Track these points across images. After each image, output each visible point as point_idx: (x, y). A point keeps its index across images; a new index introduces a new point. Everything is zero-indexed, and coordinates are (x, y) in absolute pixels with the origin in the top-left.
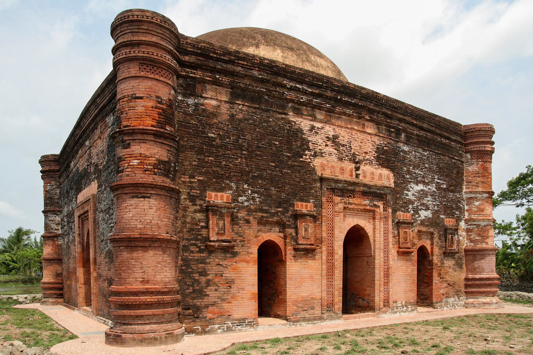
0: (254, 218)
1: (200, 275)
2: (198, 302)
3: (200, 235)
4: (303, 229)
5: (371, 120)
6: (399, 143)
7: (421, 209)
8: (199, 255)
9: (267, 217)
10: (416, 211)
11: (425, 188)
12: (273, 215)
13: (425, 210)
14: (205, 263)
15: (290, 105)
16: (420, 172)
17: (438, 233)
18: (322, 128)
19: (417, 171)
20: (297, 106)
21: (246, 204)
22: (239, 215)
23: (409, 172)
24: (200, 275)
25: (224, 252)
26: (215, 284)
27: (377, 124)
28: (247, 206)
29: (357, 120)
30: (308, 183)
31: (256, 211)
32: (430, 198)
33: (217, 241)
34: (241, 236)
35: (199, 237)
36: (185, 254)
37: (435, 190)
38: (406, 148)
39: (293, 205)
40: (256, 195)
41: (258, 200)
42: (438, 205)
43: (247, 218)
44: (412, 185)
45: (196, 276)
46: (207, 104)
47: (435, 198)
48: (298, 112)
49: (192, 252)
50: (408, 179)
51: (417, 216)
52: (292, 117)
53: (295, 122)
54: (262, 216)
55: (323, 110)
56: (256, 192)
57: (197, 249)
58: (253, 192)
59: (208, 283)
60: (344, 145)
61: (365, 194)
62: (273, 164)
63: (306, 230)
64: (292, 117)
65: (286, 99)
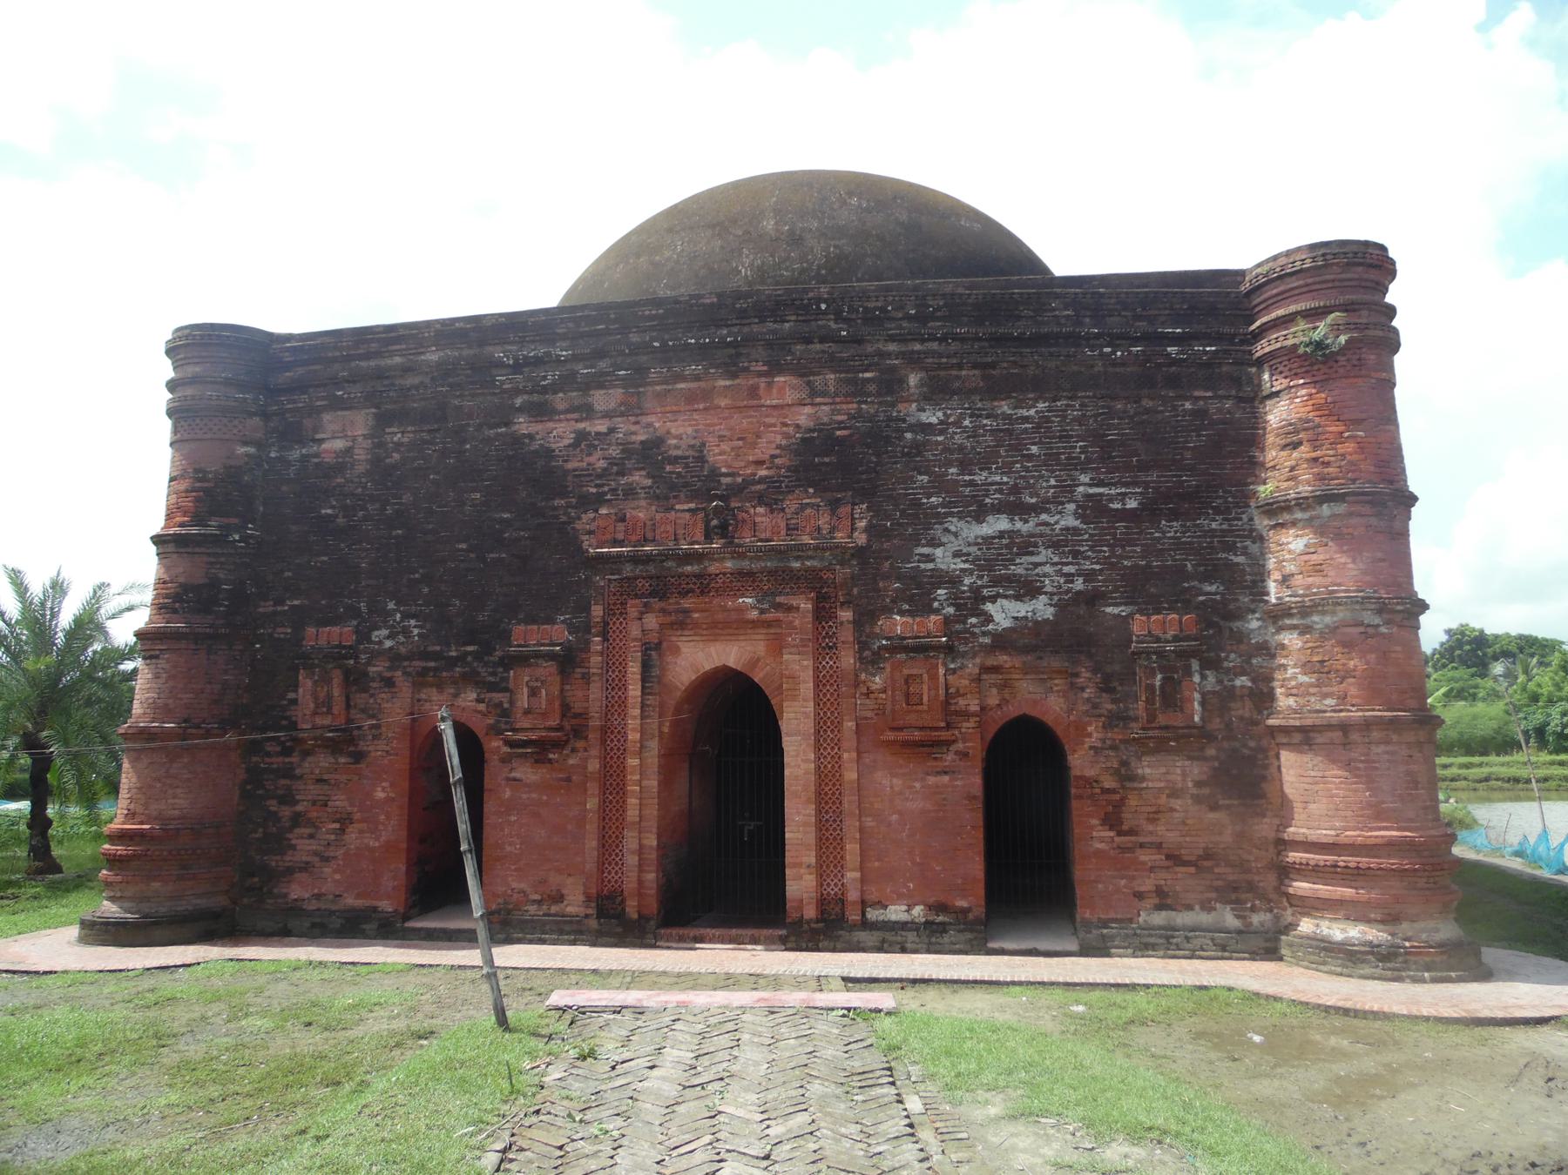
0: (405, 673)
1: (280, 803)
2: (273, 861)
3: (286, 718)
4: (525, 690)
5: (775, 368)
6: (901, 406)
7: (993, 599)
8: (280, 759)
9: (435, 669)
10: (973, 604)
11: (1019, 525)
12: (453, 662)
13: (1018, 598)
14: (294, 777)
15: (518, 401)
16: (998, 478)
17: (1095, 671)
18: (612, 430)
19: (980, 477)
20: (535, 397)
21: (388, 644)
22: (372, 669)
23: (940, 484)
24: (280, 803)
25: (333, 753)
27: (802, 376)
28: (391, 648)
29: (728, 383)
31: (410, 657)
32: (1044, 554)
34: (373, 717)
35: (284, 722)
36: (254, 759)
37: (1077, 523)
38: (932, 417)
39: (506, 637)
40: (413, 622)
41: (416, 631)
42: (1089, 576)
43: (388, 674)
44: (954, 524)
45: (273, 805)
46: (326, 451)
47: (1076, 554)
48: (541, 411)
49: (268, 754)
50: (936, 507)
51: (973, 620)
53: (531, 437)
54: (426, 670)
55: (616, 386)
56: (413, 616)
57: (278, 749)
58: (406, 616)
59: (297, 820)
60: (677, 458)
62: (464, 546)
63: (534, 693)
64: (523, 425)
65: (505, 391)
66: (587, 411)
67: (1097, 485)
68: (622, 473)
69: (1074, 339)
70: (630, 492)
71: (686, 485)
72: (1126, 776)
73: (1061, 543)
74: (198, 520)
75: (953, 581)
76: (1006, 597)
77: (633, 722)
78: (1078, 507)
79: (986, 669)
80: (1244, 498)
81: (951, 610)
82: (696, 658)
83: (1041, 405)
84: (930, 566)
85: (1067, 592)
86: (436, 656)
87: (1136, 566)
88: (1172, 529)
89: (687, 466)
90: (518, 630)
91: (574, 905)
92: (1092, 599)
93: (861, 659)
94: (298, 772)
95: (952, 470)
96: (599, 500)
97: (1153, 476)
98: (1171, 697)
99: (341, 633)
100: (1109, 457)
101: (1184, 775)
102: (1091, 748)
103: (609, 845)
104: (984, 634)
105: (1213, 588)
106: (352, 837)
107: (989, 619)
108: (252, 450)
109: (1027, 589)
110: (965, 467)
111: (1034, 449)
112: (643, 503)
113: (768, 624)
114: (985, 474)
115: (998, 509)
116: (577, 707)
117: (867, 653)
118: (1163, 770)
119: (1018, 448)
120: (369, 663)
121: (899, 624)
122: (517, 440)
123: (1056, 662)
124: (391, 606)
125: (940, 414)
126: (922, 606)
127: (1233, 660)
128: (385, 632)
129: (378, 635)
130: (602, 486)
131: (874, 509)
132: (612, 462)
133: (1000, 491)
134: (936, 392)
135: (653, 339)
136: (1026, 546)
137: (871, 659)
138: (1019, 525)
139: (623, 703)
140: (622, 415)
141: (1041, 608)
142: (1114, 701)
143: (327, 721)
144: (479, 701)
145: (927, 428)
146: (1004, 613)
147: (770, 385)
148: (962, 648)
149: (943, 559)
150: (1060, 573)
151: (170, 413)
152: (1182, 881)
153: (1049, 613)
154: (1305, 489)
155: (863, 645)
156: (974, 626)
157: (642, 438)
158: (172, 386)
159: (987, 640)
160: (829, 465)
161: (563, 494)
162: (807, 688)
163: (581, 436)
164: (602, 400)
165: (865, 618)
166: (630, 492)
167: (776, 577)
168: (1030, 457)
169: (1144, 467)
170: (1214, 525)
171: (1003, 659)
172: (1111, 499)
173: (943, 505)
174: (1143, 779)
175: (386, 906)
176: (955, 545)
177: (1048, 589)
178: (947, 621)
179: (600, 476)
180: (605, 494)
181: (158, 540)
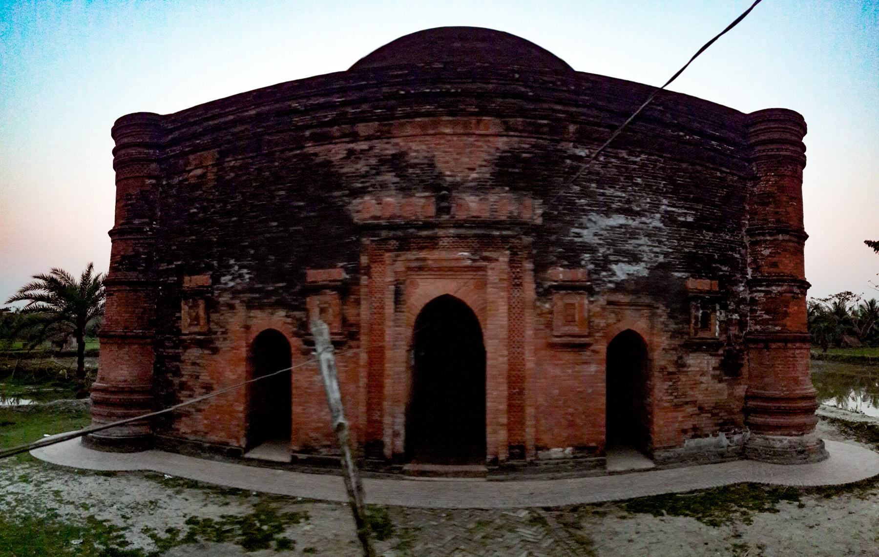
0: (241, 302)
11: (630, 222)
16: (619, 194)
17: (667, 307)
26: (190, 389)
28: (232, 287)
32: (644, 240)
33: (190, 334)
37: (661, 225)
40: (245, 271)
42: (666, 255)
59: (183, 386)
67: (672, 206)
68: (378, 174)
70: (384, 186)
71: (422, 181)
72: (680, 365)
76: (624, 262)
78: (662, 216)
79: (610, 303)
81: (591, 266)
83: (643, 156)
84: (580, 240)
85: (655, 262)
86: (258, 291)
87: (690, 252)
89: (422, 169)
93: (538, 293)
94: (183, 358)
95: (593, 185)
97: (700, 207)
98: (705, 323)
99: (203, 280)
100: (677, 192)
101: (708, 363)
102: (664, 349)
104: (610, 282)
105: (726, 269)
107: (614, 274)
108: (154, 181)
109: (634, 258)
111: (639, 180)
112: (393, 193)
113: (479, 269)
114: (612, 190)
116: (352, 319)
117: (541, 290)
118: (699, 361)
119: (630, 178)
120: (219, 296)
121: (559, 273)
122: (307, 157)
123: (647, 300)
124: (232, 262)
125: (587, 151)
128: (229, 277)
129: (224, 279)
130: (366, 182)
132: (372, 167)
133: (620, 201)
135: (399, 90)
136: (633, 234)
137: (544, 293)
138: (630, 222)
140: (378, 138)
141: (640, 270)
142: (676, 324)
143: (197, 329)
144: (287, 316)
145: (579, 158)
146: (622, 271)
147: (479, 122)
148: (597, 289)
149: (588, 236)
150: (651, 251)
153: (645, 273)
155: (539, 285)
156: (604, 276)
157: (393, 152)
159: (611, 285)
161: (339, 187)
162: (503, 309)
163: (351, 152)
164: (362, 129)
166: (384, 186)
168: (637, 185)
169: (697, 200)
170: (727, 237)
172: (680, 215)
173: (586, 205)
174: (690, 366)
176: (594, 229)
177: (645, 259)
178: (590, 273)
179: (363, 176)
180: (367, 187)
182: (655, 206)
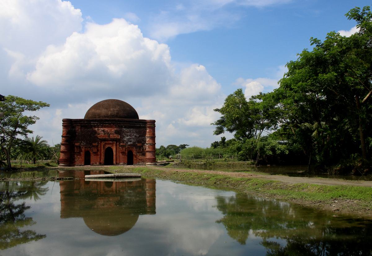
10: (127, 143)
23: (125, 134)
30: (96, 139)
52: (93, 128)
61: (110, 141)
66: (98, 127)
69: (135, 124)
73: (133, 139)
74: (67, 134)
75: (126, 141)
77: (102, 151)
80: (145, 136)
82: (107, 146)
88: (141, 138)
90: (93, 144)
91: (98, 164)
92: (135, 142)
96: (99, 134)
103: (100, 160)
106: (80, 159)
109: (131, 142)
110: (127, 133)
115: (129, 136)
119: (130, 132)
123: (132, 147)
126: (124, 143)
127: (144, 147)
131: (121, 136)
134: (125, 128)
139: (102, 149)
141: (132, 143)
146: (129, 143)
149: (125, 139)
151: (63, 126)
152: (140, 161)
154: (149, 136)
158: (63, 124)
160: (116, 132)
164: (100, 126)
165: (120, 143)
167: (113, 140)
169: (139, 133)
171: (129, 146)
175: (83, 164)
181: (62, 136)
182: (134, 135)
